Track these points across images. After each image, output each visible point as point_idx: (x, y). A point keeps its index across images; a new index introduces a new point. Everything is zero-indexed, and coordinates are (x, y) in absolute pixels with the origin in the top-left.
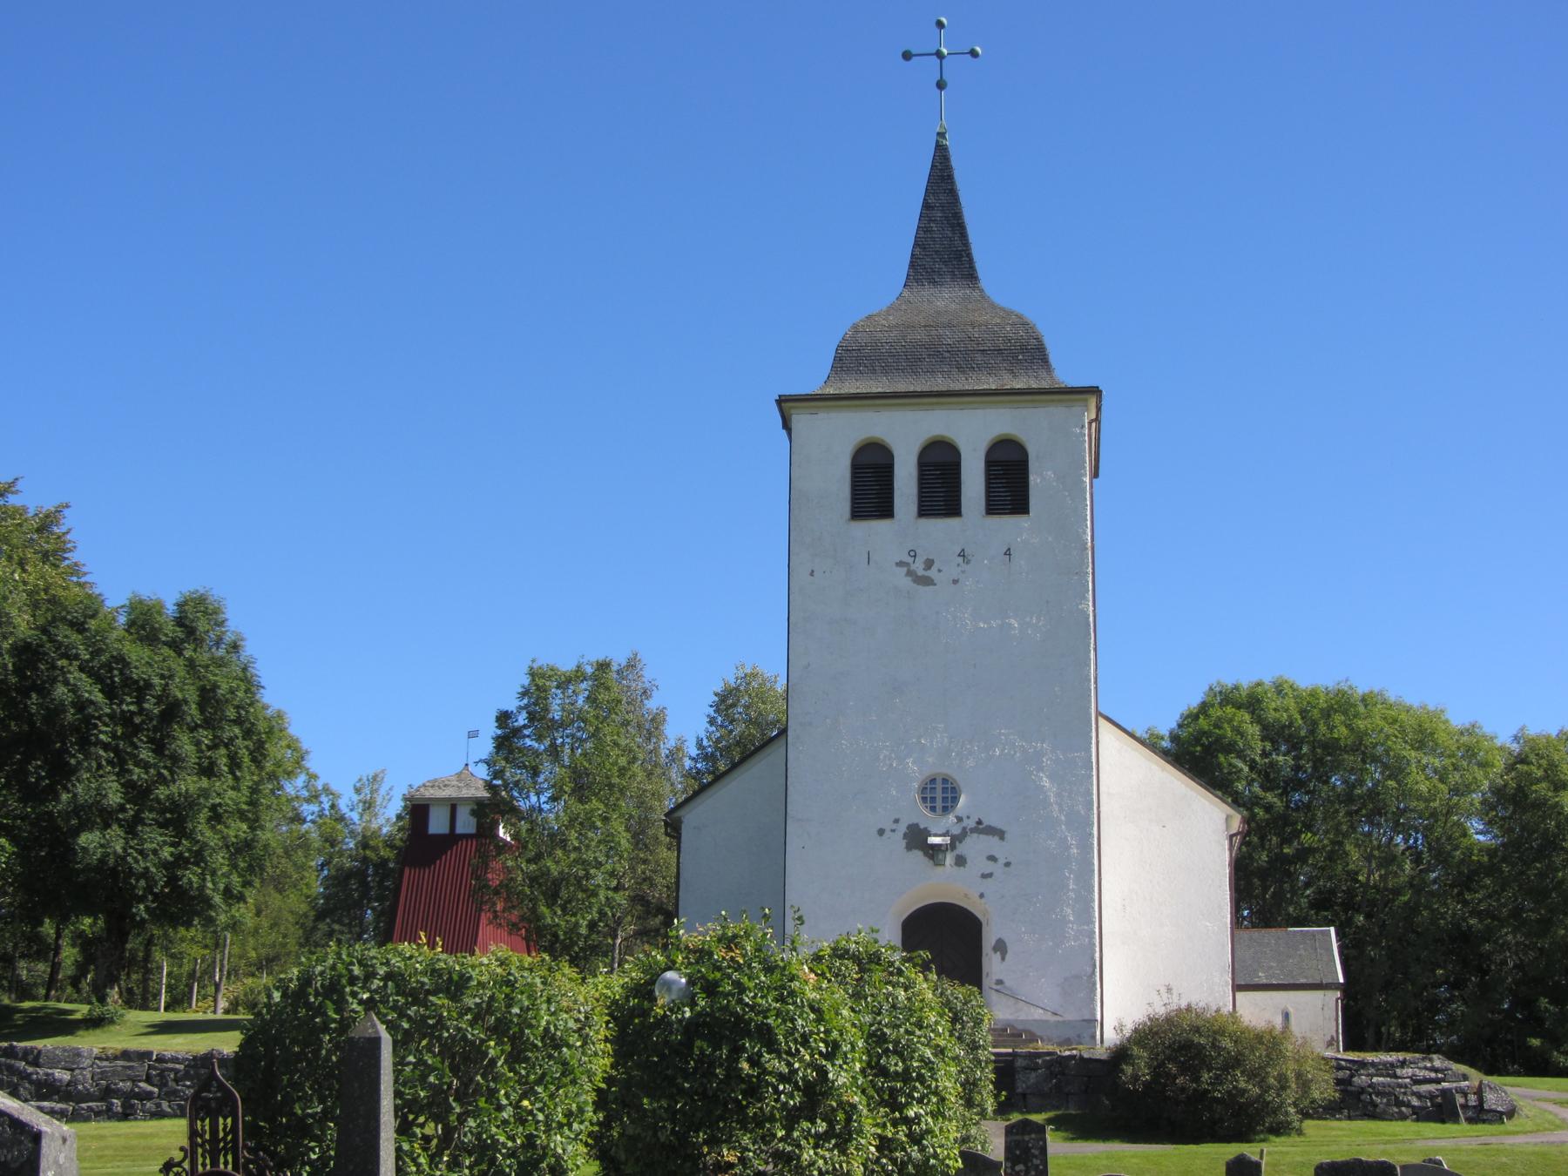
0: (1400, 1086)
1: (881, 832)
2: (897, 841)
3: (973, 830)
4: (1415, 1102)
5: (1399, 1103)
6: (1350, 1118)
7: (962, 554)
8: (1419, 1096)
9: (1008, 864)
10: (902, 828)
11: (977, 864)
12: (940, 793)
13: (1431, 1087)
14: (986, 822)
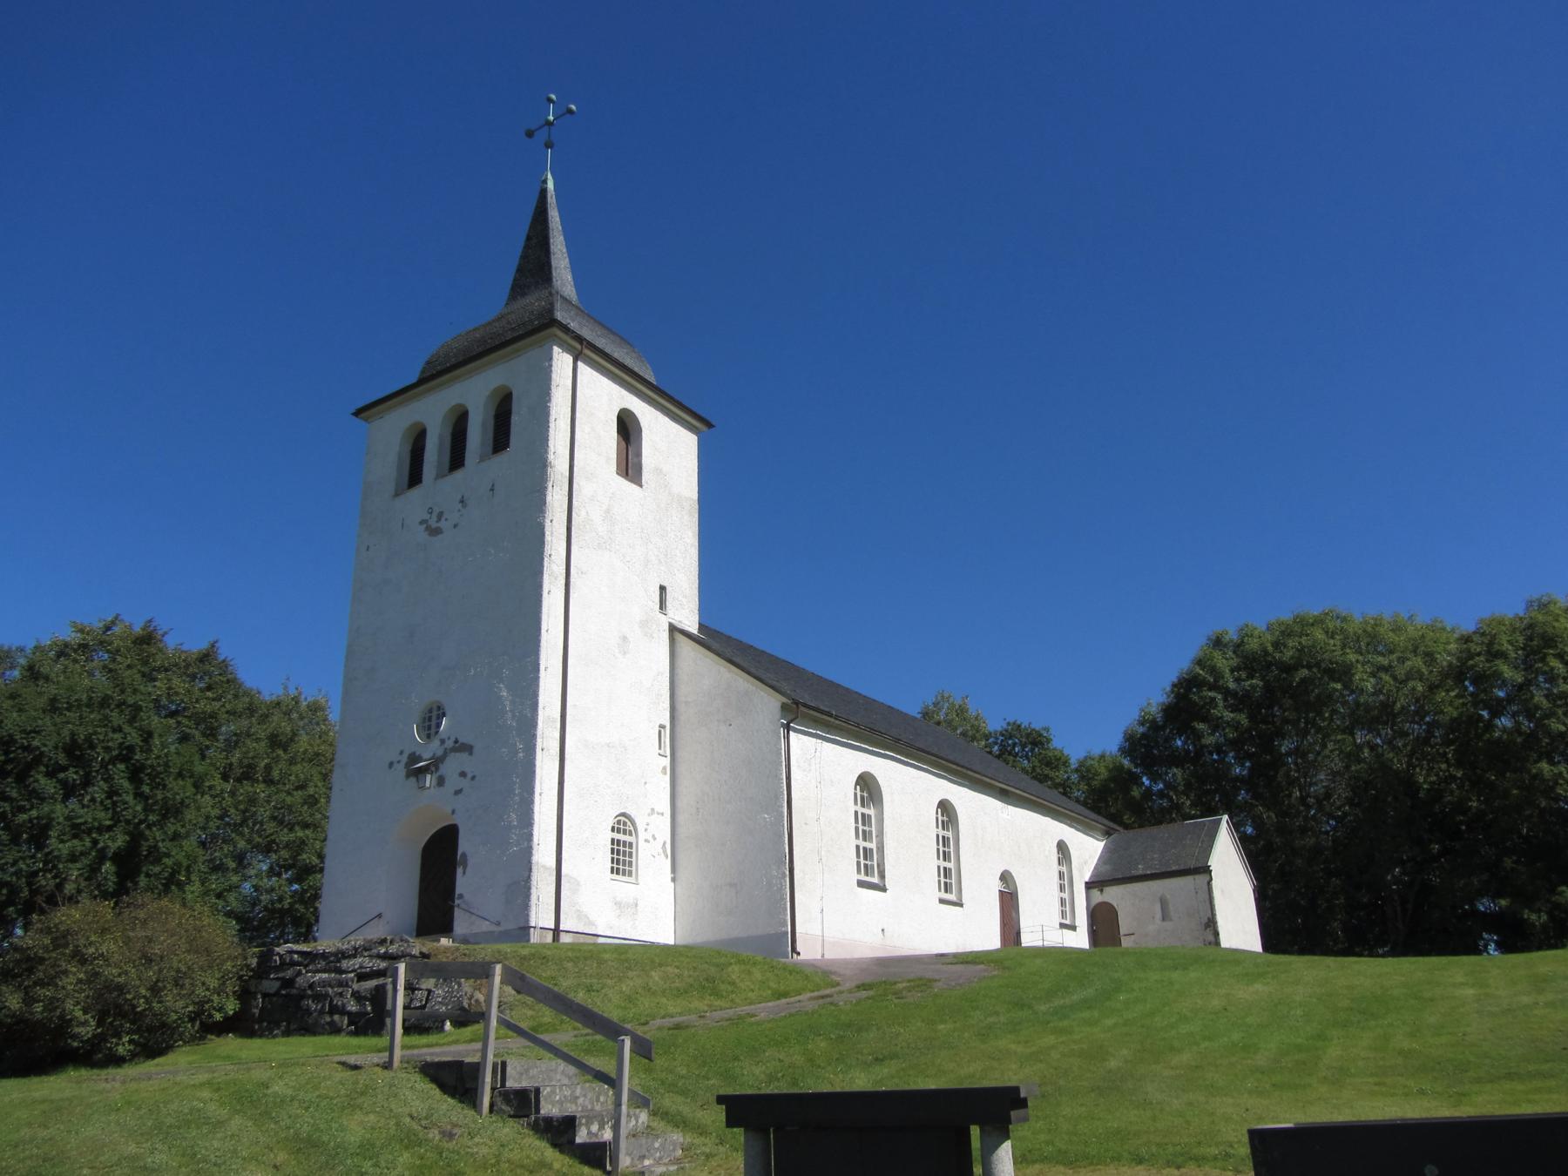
0: (341, 984)
1: (391, 765)
2: (400, 770)
3: (454, 750)
4: (352, 1007)
5: (334, 1010)
6: (287, 1033)
7: (462, 501)
8: (357, 996)
9: (473, 778)
10: (404, 759)
11: (453, 781)
12: (431, 720)
13: (373, 983)
14: (461, 740)
